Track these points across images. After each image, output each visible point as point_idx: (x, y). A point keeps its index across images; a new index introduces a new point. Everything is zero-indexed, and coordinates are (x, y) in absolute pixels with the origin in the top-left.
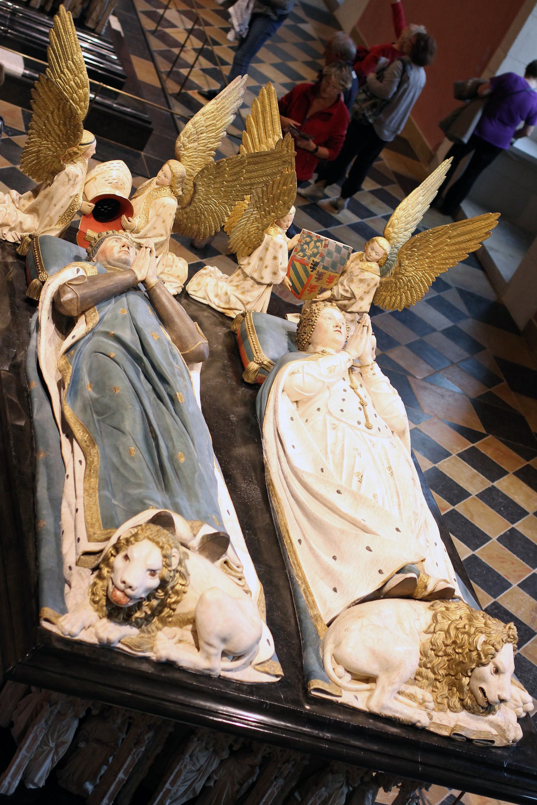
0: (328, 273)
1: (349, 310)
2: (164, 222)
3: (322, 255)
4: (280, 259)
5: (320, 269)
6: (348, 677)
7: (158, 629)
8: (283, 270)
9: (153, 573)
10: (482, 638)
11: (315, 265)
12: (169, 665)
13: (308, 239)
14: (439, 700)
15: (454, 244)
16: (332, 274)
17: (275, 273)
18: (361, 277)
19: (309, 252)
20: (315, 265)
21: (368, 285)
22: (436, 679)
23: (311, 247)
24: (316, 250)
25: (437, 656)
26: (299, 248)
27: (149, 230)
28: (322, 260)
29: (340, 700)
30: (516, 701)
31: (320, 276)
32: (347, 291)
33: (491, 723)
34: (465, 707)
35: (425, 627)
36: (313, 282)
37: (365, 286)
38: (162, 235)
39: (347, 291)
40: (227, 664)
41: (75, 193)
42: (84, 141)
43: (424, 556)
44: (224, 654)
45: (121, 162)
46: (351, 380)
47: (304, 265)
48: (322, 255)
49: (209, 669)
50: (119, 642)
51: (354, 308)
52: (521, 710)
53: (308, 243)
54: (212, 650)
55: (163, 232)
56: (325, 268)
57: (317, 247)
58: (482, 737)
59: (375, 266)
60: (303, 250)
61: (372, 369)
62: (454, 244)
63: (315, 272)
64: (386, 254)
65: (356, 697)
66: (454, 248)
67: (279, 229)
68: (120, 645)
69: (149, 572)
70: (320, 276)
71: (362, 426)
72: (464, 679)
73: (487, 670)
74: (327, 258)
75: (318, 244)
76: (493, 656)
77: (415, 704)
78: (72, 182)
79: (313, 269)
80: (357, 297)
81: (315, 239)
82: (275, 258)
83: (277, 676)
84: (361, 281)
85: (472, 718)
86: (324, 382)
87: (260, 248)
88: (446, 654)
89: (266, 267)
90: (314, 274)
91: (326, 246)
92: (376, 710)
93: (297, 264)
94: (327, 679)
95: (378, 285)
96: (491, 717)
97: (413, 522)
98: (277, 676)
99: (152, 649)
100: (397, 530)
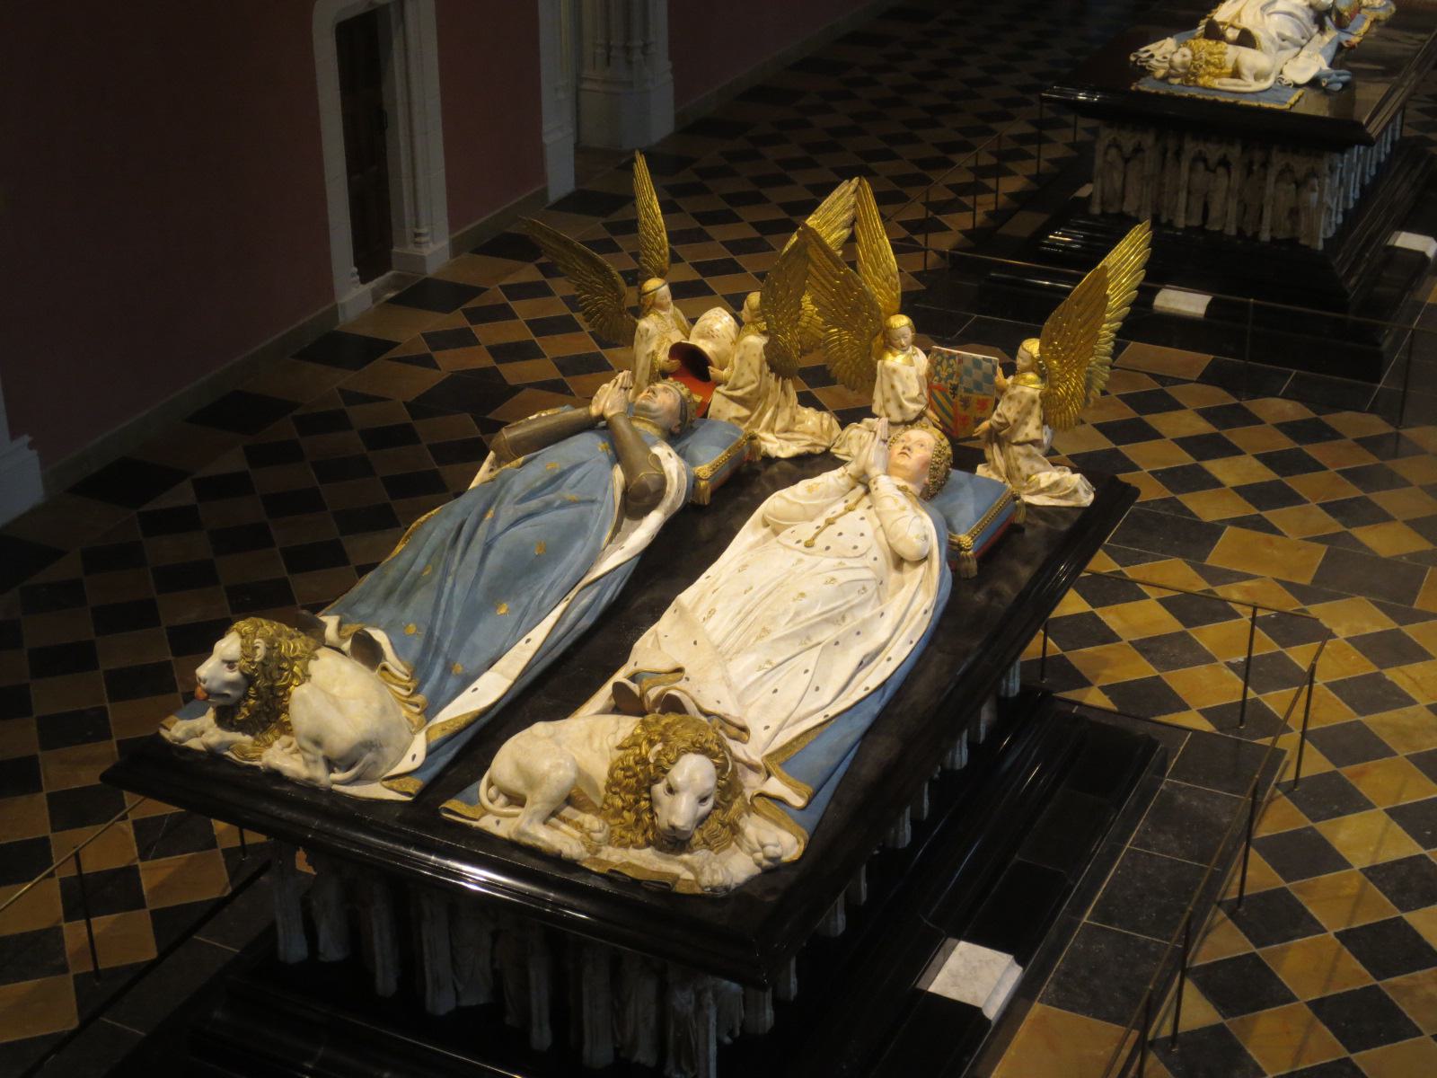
0: (976, 396)
1: (1014, 441)
2: (750, 364)
3: (959, 375)
4: (900, 388)
5: (961, 392)
6: (502, 799)
7: (277, 738)
8: (914, 400)
9: (230, 664)
10: (659, 747)
11: (955, 388)
12: (275, 775)
13: (939, 358)
14: (623, 833)
15: (1085, 323)
16: (981, 397)
17: (901, 407)
18: (1012, 392)
19: (944, 374)
20: (955, 388)
21: (1020, 402)
22: (623, 808)
23: (945, 367)
24: (950, 370)
25: (626, 777)
26: (933, 371)
27: (736, 378)
28: (961, 381)
29: (475, 824)
30: (750, 842)
31: (966, 403)
32: (999, 415)
33: (690, 868)
34: (648, 844)
35: (619, 741)
36: (961, 412)
37: (1016, 404)
38: (753, 382)
39: (999, 415)
40: (338, 776)
41: (650, 350)
42: (648, 289)
43: (682, 664)
44: (331, 764)
45: (719, 309)
46: (857, 502)
47: (942, 391)
48: (959, 375)
49: (309, 779)
50: (228, 750)
51: (1020, 438)
52: (759, 856)
53: (940, 363)
54: (308, 756)
55: (753, 377)
56: (967, 390)
57: (951, 366)
58: (655, 878)
59: (1031, 376)
60: (937, 373)
61: (875, 483)
62: (1085, 323)
63: (958, 398)
64: (1032, 357)
65: (498, 822)
66: (1086, 328)
67: (898, 352)
68: (228, 753)
69: (225, 665)
70: (966, 403)
71: (801, 546)
72: (643, 803)
73: (659, 789)
74: (965, 377)
75: (952, 361)
76: (666, 772)
77: (577, 834)
78: (645, 338)
79: (954, 394)
80: (1011, 421)
81: (946, 356)
82: (893, 387)
83: (409, 794)
84: (1010, 398)
85: (658, 857)
86: (801, 505)
87: (878, 379)
88: (635, 775)
89: (888, 400)
90: (957, 400)
91: (961, 361)
92: (514, 837)
93: (937, 393)
94: (473, 801)
95: (1039, 401)
96: (686, 857)
97: (753, 639)
98: (409, 794)
99: (259, 758)
100: (695, 643)
